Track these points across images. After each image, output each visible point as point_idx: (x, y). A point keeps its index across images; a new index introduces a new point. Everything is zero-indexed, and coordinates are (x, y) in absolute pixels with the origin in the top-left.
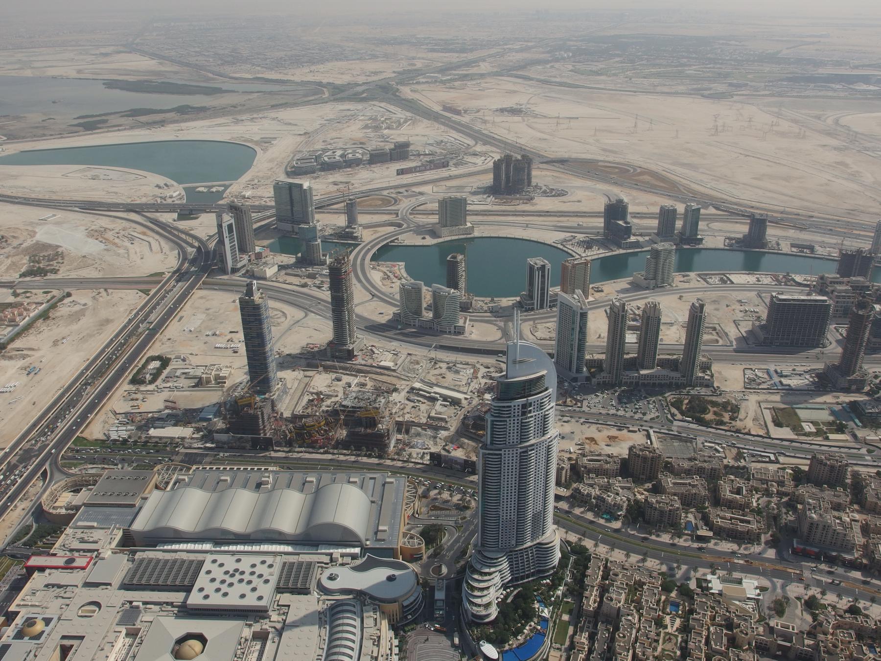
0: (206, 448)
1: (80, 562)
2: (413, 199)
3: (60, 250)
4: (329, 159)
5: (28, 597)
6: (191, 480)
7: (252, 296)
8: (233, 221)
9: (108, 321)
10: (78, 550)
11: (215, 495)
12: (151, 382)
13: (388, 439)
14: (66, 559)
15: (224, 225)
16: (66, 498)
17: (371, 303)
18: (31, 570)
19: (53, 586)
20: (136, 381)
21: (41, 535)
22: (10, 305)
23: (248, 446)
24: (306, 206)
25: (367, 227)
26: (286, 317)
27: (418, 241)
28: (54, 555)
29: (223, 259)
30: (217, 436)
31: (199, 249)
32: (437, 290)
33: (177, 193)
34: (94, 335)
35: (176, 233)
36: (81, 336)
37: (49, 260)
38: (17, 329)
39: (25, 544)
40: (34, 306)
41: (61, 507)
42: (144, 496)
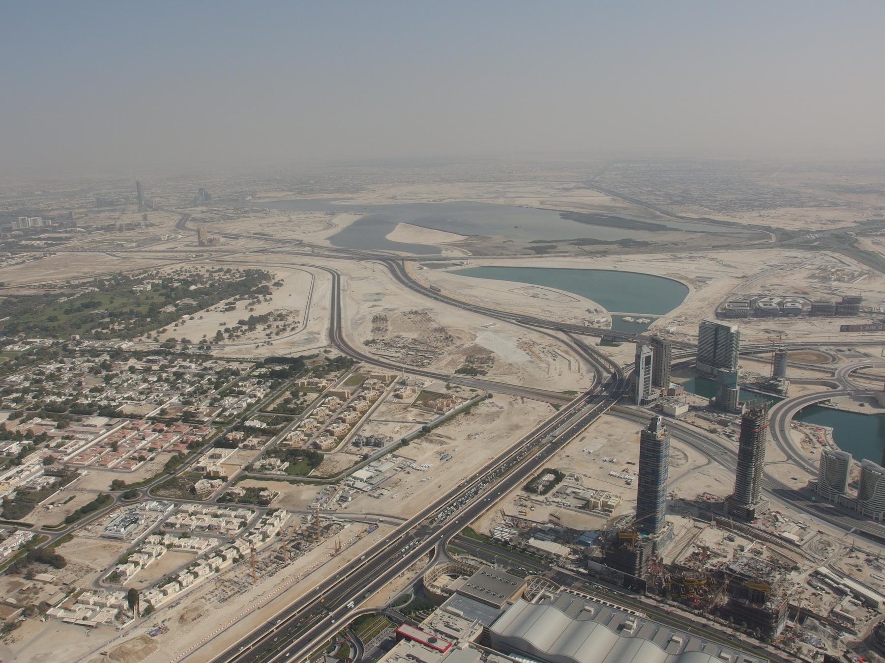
0: (578, 572)
1: (441, 644)
2: (856, 360)
3: (492, 355)
4: (764, 305)
5: (392, 660)
6: (556, 599)
7: (655, 431)
8: (651, 354)
9: (517, 427)
10: (442, 633)
11: (575, 622)
12: (543, 493)
13: (776, 622)
14: (430, 637)
15: (642, 356)
16: (444, 580)
17: (785, 465)
18: (400, 636)
19: (414, 658)
20: (530, 488)
21: (415, 607)
22: (442, 396)
23: (620, 582)
24: (731, 351)
25: (794, 382)
26: (687, 460)
27: (854, 407)
28: (421, 629)
29: (634, 389)
30: (591, 563)
31: (614, 375)
32: (869, 467)
33: (605, 319)
34: (502, 437)
35: (596, 356)
36: (491, 436)
37: (482, 363)
38: (442, 417)
39: (401, 611)
40: (460, 400)
41: (438, 587)
42: (510, 601)
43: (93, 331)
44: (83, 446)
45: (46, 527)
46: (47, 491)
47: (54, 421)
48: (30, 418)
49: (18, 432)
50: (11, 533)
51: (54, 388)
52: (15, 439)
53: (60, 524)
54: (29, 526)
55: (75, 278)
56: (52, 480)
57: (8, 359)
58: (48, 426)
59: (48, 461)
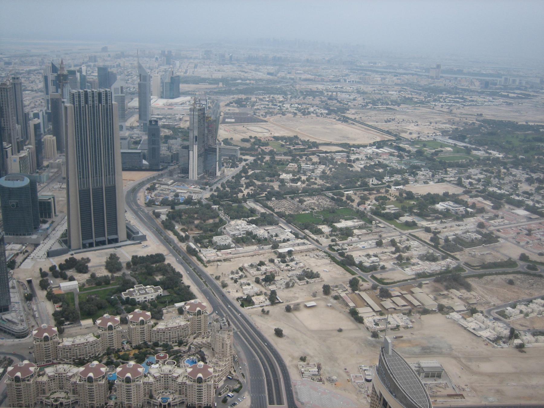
43: (536, 157)
44: (506, 225)
45: (466, 264)
46: (473, 243)
47: (492, 203)
48: (476, 196)
49: (466, 202)
50: (444, 258)
51: (497, 183)
52: (464, 205)
53: (477, 266)
54: (457, 259)
55: (532, 122)
56: (479, 237)
57: (473, 159)
58: (488, 204)
59: (481, 225)
